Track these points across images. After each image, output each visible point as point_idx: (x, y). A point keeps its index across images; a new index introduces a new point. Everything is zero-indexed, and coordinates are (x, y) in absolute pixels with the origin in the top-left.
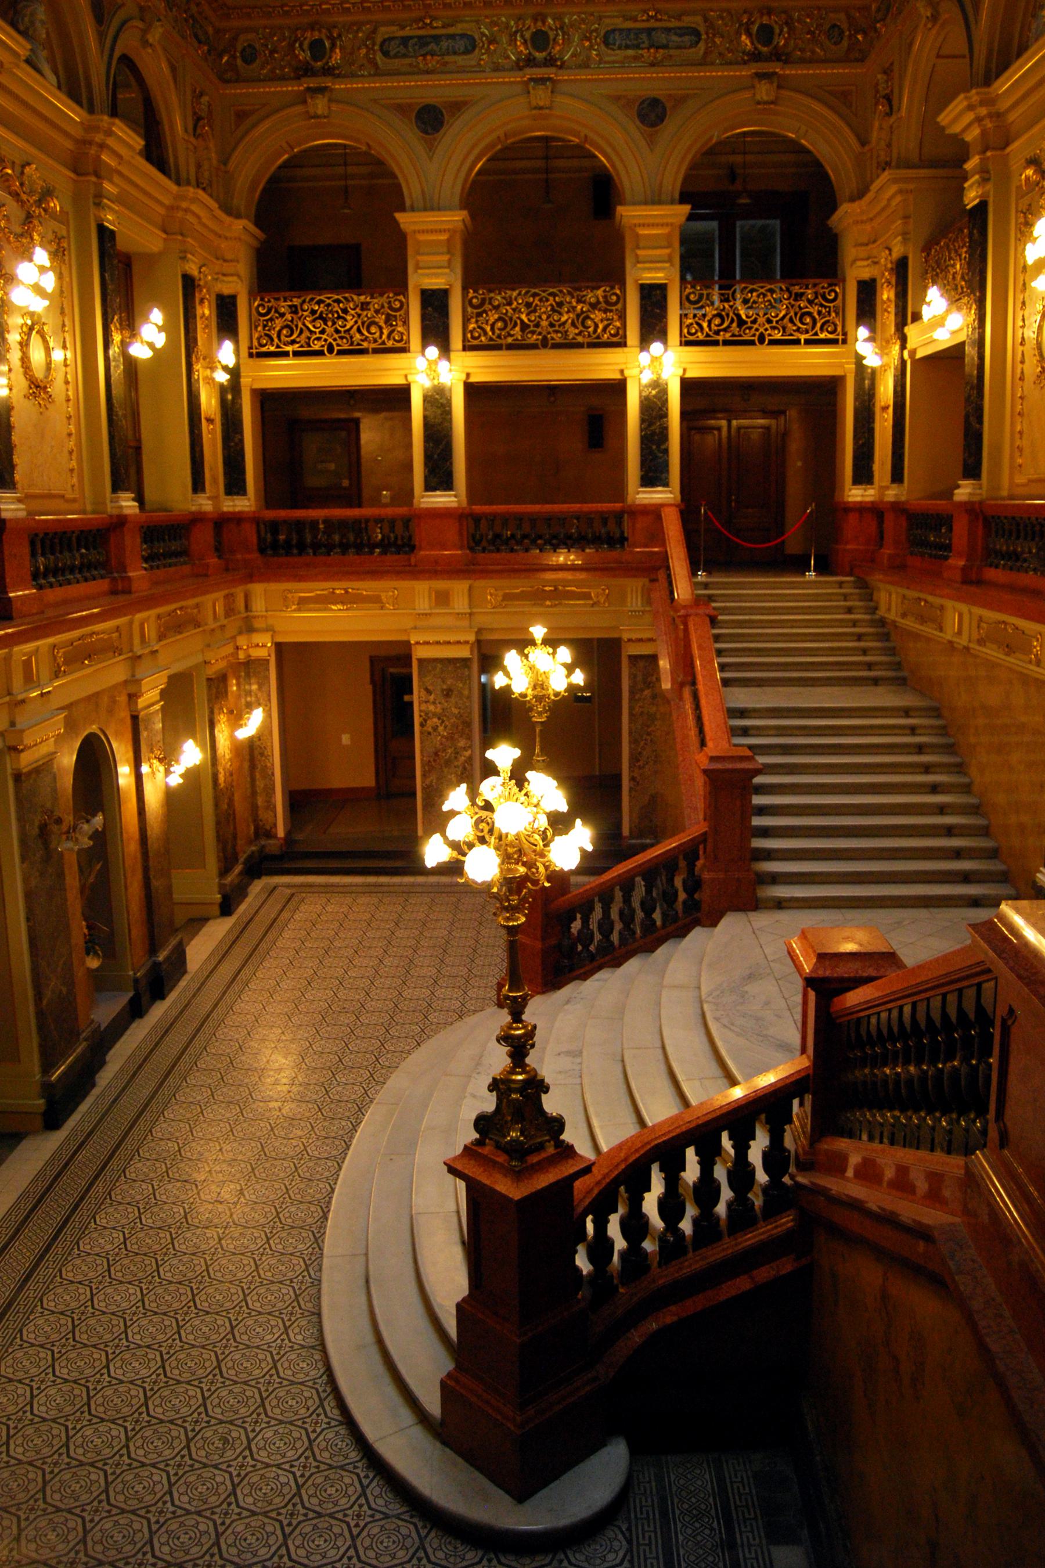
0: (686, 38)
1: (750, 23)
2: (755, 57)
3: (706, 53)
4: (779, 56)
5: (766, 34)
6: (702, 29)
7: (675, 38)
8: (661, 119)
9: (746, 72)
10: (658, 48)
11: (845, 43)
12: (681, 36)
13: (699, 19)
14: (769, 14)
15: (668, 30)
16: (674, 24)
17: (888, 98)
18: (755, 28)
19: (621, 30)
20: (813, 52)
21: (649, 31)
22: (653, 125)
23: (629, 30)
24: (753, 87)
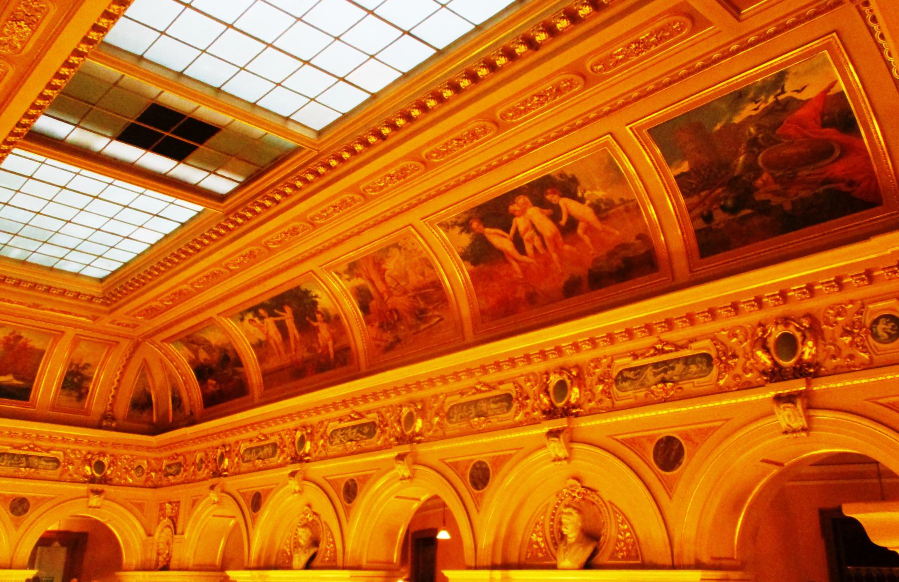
0: (51, 464)
1: (92, 459)
2: (92, 480)
3: (61, 474)
4: (105, 480)
5: (100, 466)
6: (61, 460)
7: (44, 463)
8: (26, 511)
9: (83, 488)
10: (31, 468)
11: (145, 476)
12: (47, 462)
13: (61, 453)
14: (104, 456)
15: (40, 457)
16: (45, 454)
17: (174, 520)
18: (93, 462)
19: (8, 454)
20: (126, 479)
21: (27, 457)
22: (20, 514)
23: (14, 455)
24: (88, 497)
